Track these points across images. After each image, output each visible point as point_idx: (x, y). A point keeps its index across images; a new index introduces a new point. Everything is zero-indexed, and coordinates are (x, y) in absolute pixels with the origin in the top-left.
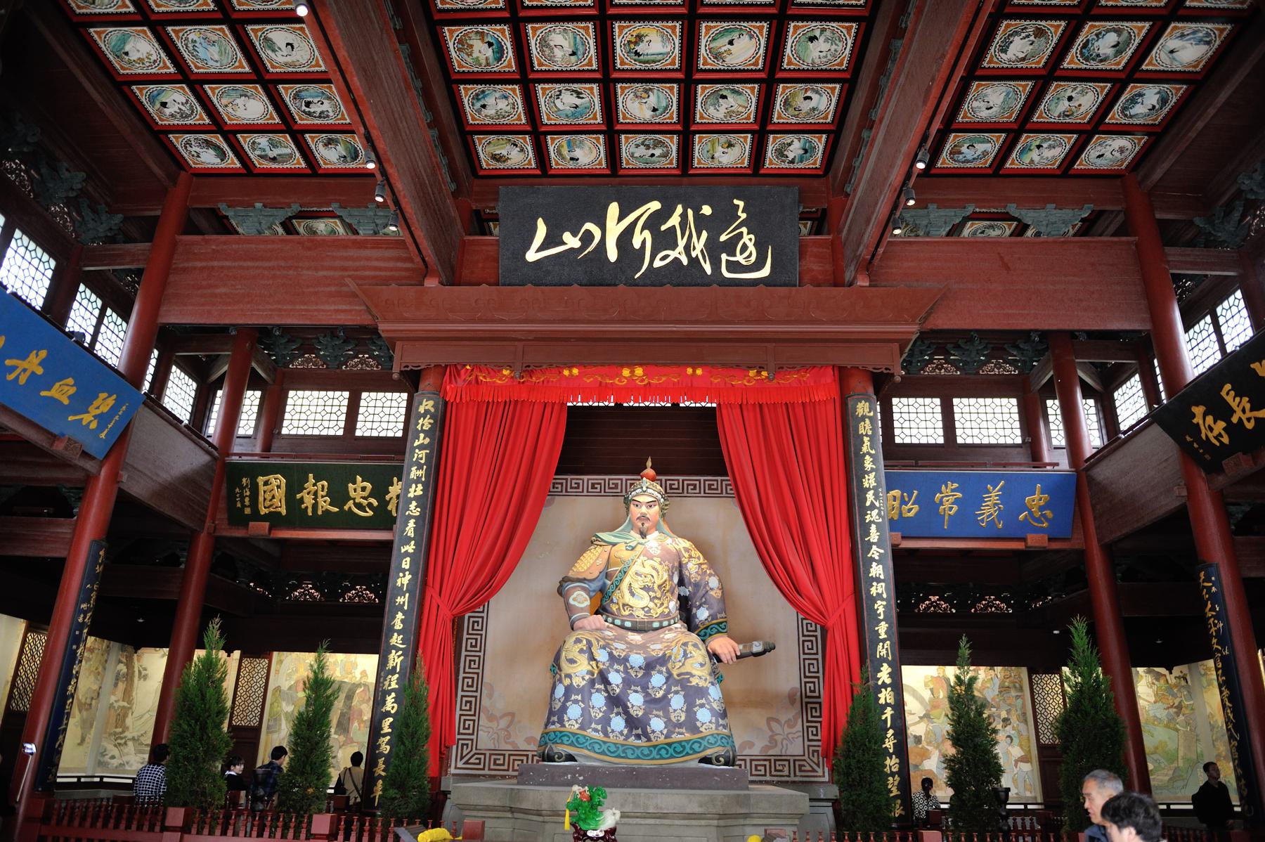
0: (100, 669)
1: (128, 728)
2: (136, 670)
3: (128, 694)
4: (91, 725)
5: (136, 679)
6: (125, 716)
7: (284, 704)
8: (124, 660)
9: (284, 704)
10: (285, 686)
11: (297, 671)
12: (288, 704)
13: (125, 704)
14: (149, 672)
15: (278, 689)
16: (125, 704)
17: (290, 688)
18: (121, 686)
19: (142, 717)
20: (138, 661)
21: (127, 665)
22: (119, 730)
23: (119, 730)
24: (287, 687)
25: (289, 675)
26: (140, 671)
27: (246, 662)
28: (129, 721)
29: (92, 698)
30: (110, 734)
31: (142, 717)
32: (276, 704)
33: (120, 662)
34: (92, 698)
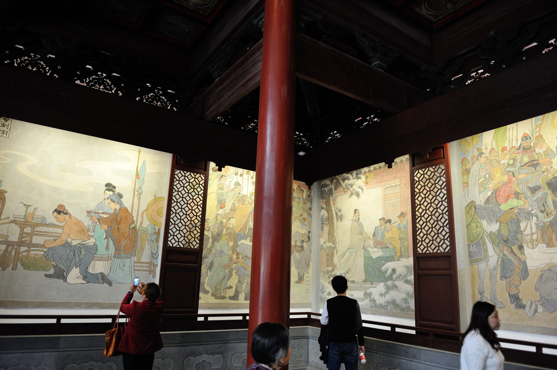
0: (305, 215)
1: (336, 266)
2: (334, 212)
3: (331, 234)
4: (308, 266)
5: (335, 220)
6: (332, 256)
7: (484, 223)
8: (324, 206)
9: (484, 223)
10: (480, 200)
11: (491, 177)
12: (490, 221)
13: (331, 244)
14: (344, 212)
15: (471, 206)
16: (331, 244)
17: (488, 201)
18: (326, 229)
19: (344, 254)
20: (334, 204)
21: (327, 210)
22: (330, 268)
23: (330, 268)
24: (483, 201)
25: (483, 186)
26: (336, 213)
27: (418, 174)
28: (336, 260)
29: (303, 241)
30: (325, 273)
31: (344, 254)
32: (473, 225)
33: (322, 208)
34: (303, 241)
